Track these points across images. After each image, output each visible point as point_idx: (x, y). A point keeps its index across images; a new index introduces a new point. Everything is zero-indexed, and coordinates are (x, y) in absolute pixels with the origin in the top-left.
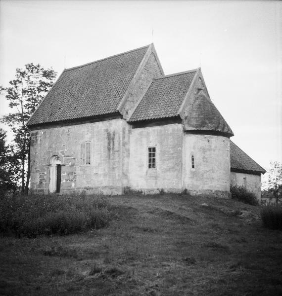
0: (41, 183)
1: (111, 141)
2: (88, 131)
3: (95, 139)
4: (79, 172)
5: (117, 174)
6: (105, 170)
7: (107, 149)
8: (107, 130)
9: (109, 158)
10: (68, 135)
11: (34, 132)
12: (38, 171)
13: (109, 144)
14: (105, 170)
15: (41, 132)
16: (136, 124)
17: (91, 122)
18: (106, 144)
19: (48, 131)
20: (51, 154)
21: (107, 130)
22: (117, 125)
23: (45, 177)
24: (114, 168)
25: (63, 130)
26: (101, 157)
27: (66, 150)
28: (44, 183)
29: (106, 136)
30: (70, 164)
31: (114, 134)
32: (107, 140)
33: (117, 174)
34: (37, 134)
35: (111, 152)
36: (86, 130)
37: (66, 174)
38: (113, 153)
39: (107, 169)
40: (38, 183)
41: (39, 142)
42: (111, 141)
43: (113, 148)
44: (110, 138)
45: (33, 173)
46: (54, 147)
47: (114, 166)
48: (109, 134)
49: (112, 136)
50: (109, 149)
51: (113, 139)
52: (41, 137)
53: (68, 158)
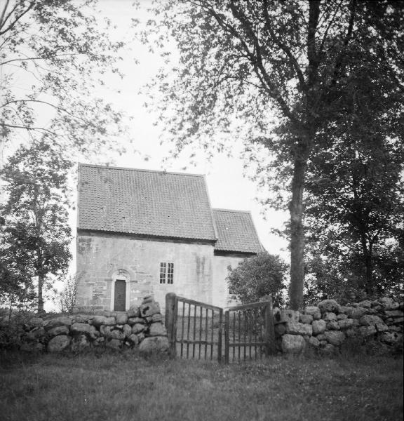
0: (96, 298)
1: (201, 265)
2: (172, 250)
3: (180, 260)
4: (158, 291)
5: (207, 297)
6: (192, 292)
7: (195, 273)
8: (195, 254)
9: (198, 281)
10: (143, 250)
11: (86, 237)
12: (93, 284)
13: (198, 267)
14: (192, 292)
15: (96, 240)
16: (218, 253)
17: (175, 242)
18: (195, 267)
19: (110, 241)
20: (115, 267)
21: (195, 254)
22: (208, 250)
23: (104, 293)
24: (204, 292)
25: (135, 245)
26: (187, 279)
27: (138, 266)
28: (102, 299)
29: (194, 259)
30: (145, 281)
31: (204, 259)
32: (196, 263)
33: (207, 297)
34: (90, 240)
35: (201, 276)
36: (168, 250)
37: (138, 291)
38: (203, 277)
39: (194, 292)
40: (91, 298)
41: (94, 251)
42: (201, 265)
43: (203, 273)
44: (200, 263)
45: (82, 286)
46: (120, 260)
47: (205, 290)
48: (198, 260)
49: (201, 260)
50: (198, 273)
51: (203, 263)
52: (97, 245)
53: (141, 274)
